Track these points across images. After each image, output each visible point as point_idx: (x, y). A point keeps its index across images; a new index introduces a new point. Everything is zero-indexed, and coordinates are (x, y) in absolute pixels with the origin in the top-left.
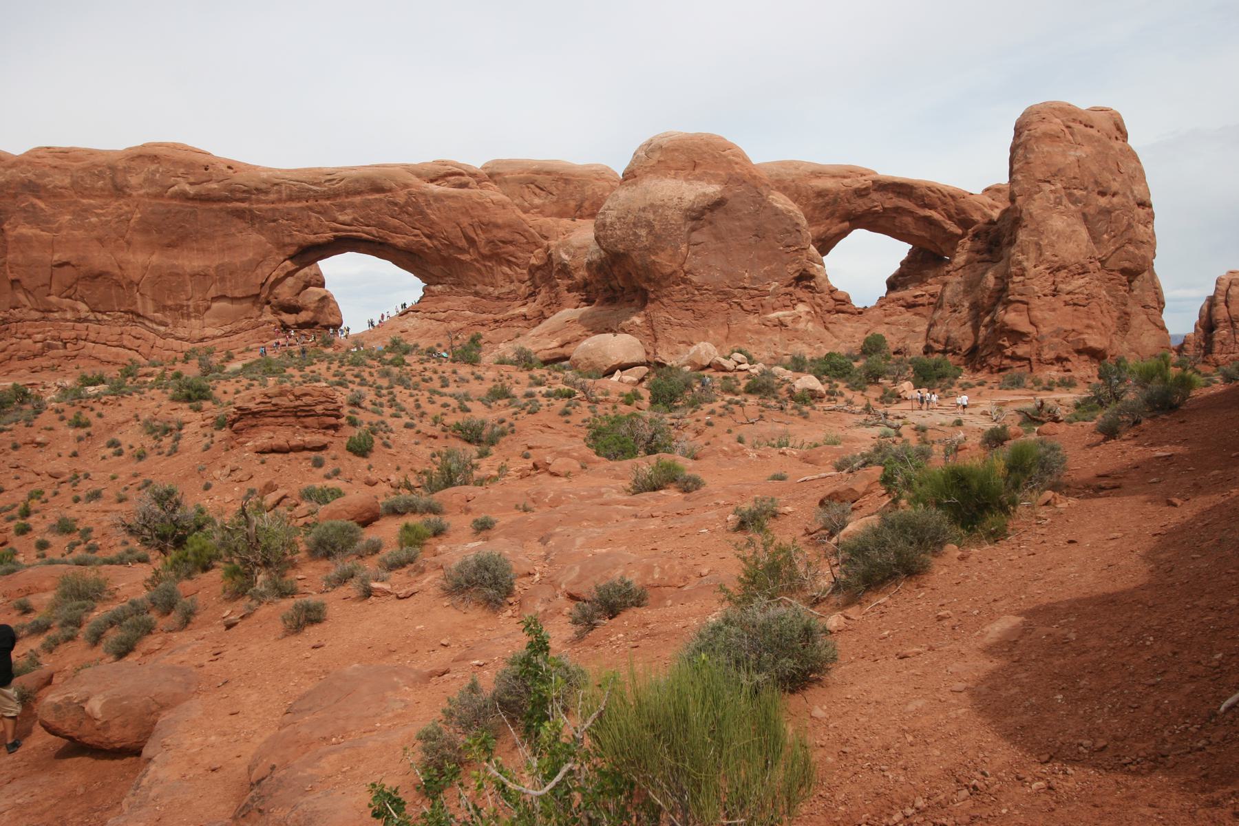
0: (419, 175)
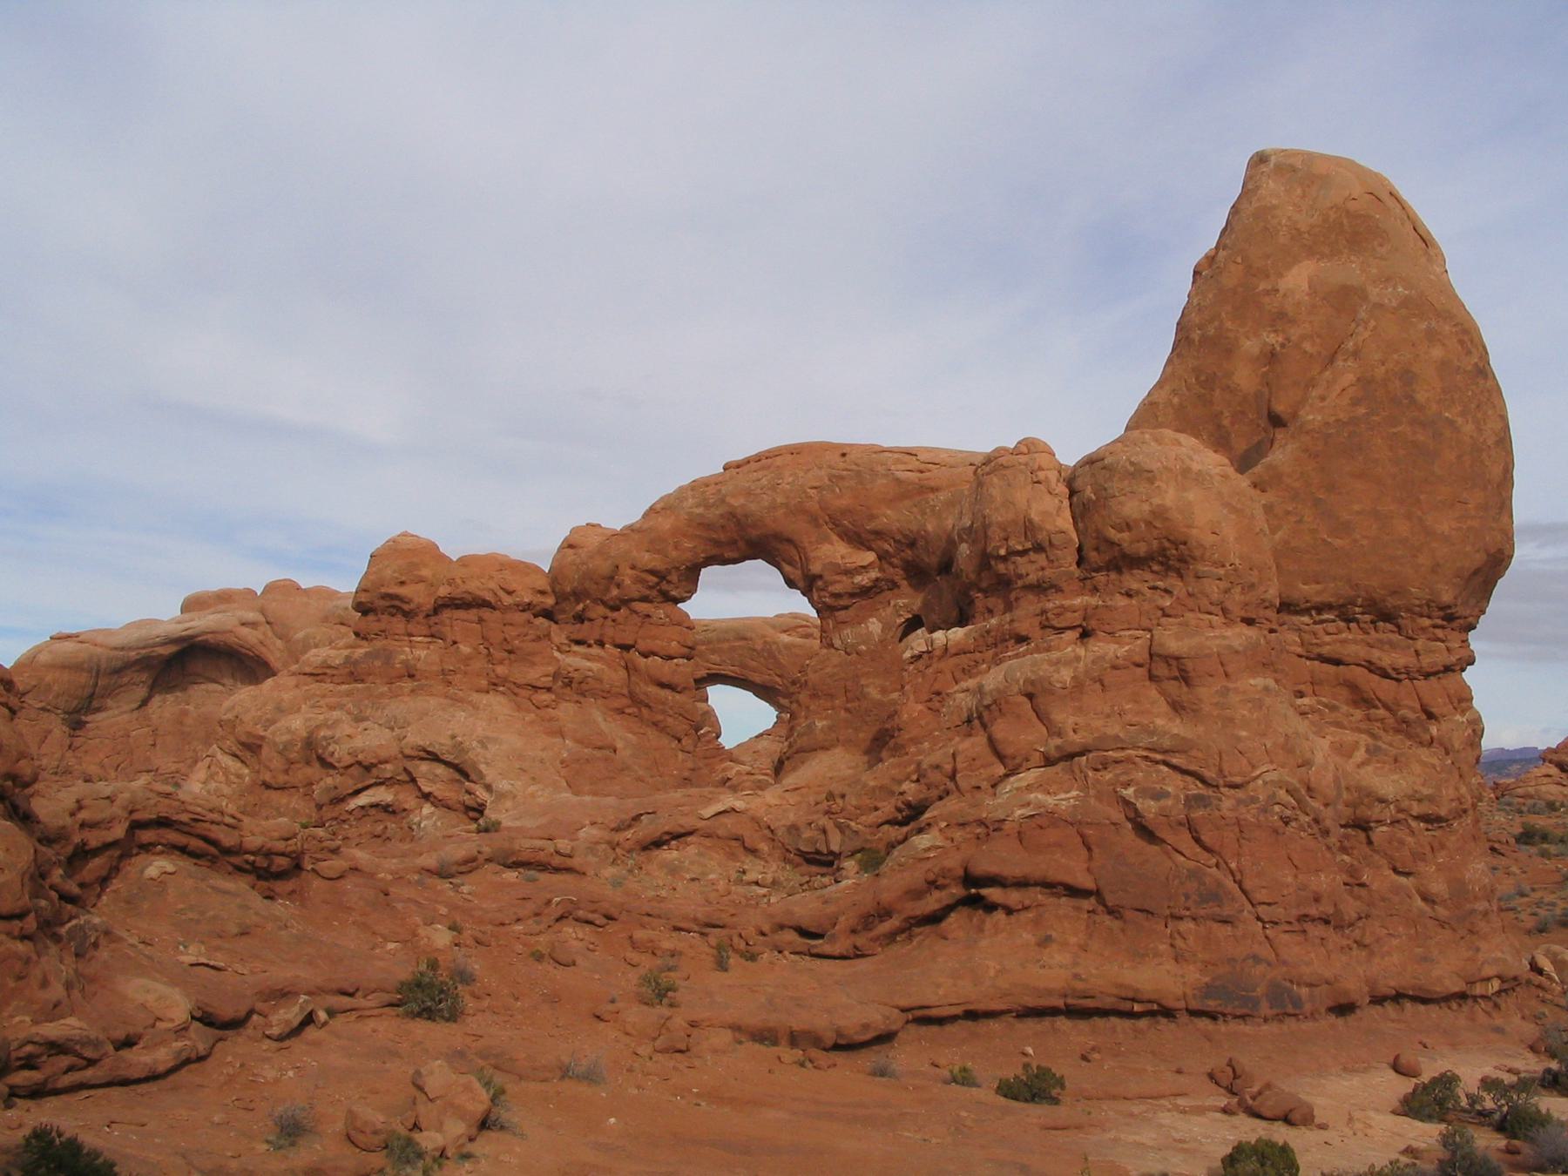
0: (774, 627)
